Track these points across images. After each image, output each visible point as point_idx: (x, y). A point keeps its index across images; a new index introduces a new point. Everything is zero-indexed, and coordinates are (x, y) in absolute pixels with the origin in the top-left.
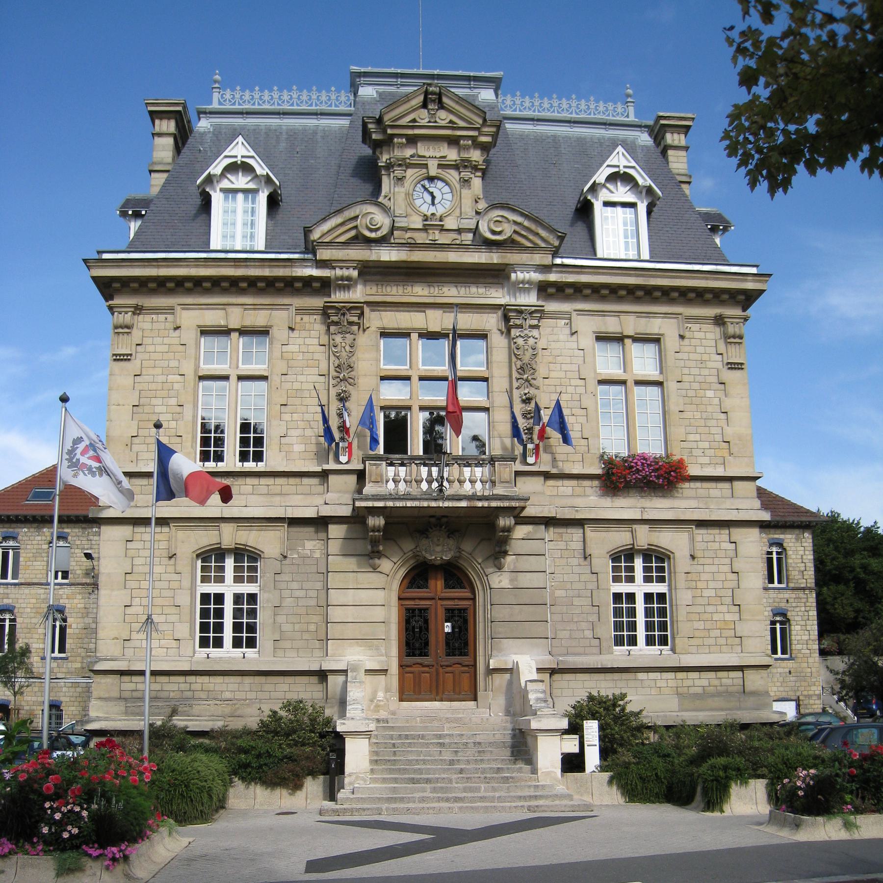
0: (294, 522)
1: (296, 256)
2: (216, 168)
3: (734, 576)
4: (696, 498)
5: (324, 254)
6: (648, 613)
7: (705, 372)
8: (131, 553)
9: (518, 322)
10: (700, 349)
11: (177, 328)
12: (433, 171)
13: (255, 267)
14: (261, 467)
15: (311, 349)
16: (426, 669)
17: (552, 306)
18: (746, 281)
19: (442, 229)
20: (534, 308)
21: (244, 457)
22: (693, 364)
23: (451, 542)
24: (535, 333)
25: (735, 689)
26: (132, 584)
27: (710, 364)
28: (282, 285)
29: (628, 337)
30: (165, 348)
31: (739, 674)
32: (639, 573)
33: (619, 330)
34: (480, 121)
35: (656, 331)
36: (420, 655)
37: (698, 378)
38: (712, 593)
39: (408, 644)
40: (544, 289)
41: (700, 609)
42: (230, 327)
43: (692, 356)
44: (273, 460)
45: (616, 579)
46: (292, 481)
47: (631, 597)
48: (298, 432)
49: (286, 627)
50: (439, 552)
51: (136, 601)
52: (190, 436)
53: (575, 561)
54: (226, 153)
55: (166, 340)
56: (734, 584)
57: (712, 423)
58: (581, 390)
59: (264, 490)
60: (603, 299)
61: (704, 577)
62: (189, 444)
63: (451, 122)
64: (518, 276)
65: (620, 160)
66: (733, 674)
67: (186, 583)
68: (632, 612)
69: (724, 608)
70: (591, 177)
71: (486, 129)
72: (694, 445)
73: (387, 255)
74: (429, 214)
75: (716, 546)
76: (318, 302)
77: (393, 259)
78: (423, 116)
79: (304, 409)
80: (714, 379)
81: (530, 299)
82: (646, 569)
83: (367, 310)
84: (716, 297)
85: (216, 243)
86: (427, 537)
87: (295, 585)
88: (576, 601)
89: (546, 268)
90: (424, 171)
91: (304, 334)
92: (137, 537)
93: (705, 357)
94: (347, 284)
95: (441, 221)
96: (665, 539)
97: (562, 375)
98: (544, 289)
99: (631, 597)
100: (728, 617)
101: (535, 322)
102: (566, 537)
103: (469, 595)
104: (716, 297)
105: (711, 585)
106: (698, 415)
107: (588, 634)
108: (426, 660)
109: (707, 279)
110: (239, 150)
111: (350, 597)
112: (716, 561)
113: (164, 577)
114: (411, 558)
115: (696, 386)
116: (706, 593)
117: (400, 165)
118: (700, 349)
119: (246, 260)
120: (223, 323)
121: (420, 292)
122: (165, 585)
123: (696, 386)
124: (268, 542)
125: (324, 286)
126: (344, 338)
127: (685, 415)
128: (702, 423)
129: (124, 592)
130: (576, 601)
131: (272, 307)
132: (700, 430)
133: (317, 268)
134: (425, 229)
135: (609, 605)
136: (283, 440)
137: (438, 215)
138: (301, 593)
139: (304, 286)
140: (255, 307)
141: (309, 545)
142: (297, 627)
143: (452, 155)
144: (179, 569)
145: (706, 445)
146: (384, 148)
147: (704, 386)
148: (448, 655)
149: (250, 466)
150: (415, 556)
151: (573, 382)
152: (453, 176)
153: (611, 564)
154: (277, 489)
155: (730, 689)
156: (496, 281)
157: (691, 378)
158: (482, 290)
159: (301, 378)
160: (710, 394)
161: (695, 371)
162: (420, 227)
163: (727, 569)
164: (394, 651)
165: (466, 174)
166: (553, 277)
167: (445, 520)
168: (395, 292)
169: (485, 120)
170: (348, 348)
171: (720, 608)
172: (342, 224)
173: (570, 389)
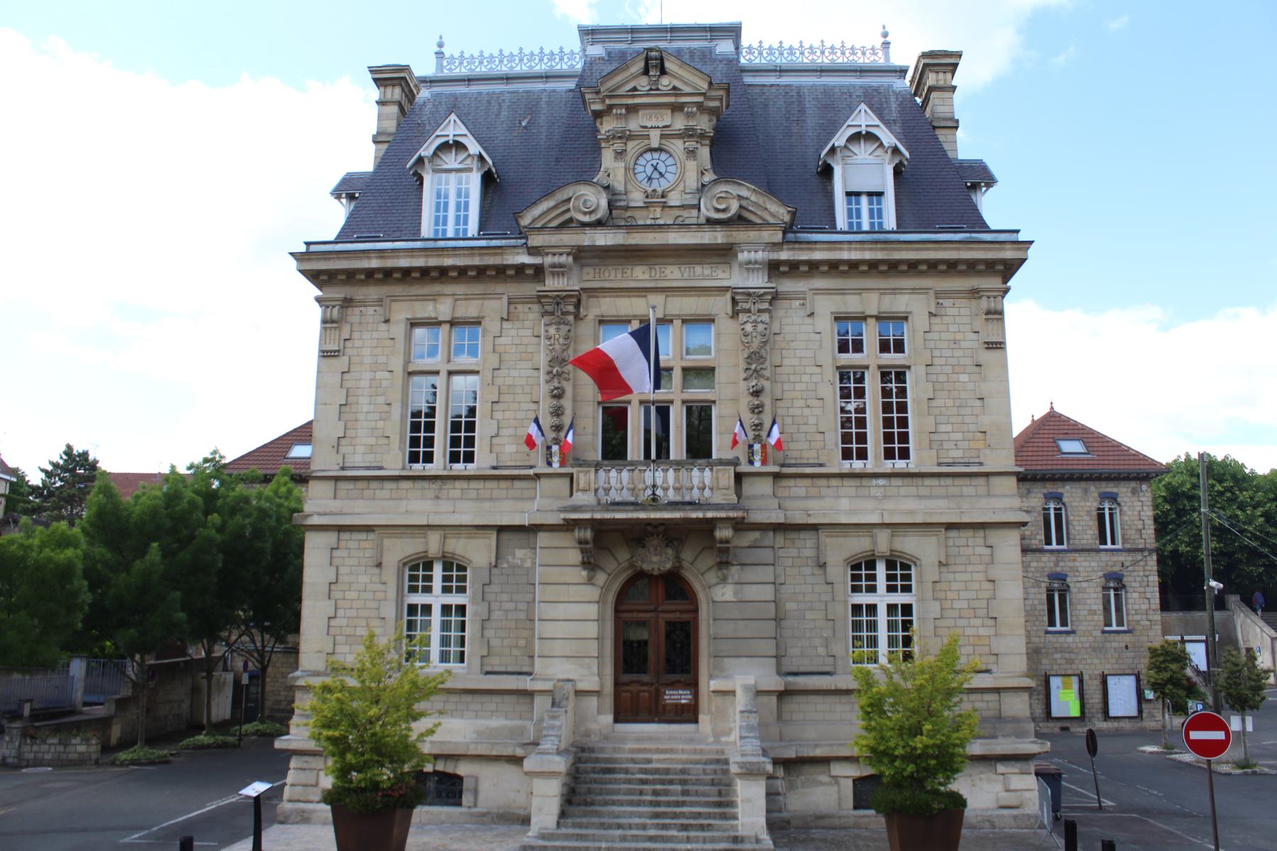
0: (501, 529)
1: (503, 242)
2: (427, 150)
3: (989, 585)
4: (947, 497)
5: (536, 240)
6: (891, 626)
7: (958, 353)
8: (336, 561)
9: (747, 306)
10: (952, 328)
11: (387, 321)
12: (655, 144)
13: (464, 255)
14: (471, 468)
15: (525, 341)
16: (645, 688)
17: (787, 285)
18: (1004, 249)
19: (665, 206)
20: (762, 291)
21: (454, 458)
22: (945, 345)
23: (670, 551)
24: (765, 317)
25: (991, 713)
26: (336, 595)
27: (964, 344)
28: (494, 273)
29: (871, 316)
30: (375, 343)
31: (994, 697)
32: (881, 582)
33: (860, 310)
34: (705, 86)
35: (902, 309)
36: (638, 672)
37: (951, 361)
38: (964, 605)
39: (625, 660)
40: (774, 268)
41: (950, 622)
42: (440, 319)
43: (944, 336)
44: (483, 461)
45: (856, 589)
46: (503, 484)
47: (872, 609)
48: (511, 431)
49: (494, 642)
50: (657, 561)
51: (341, 613)
52: (398, 437)
53: (807, 571)
54: (438, 133)
55: (375, 335)
56: (988, 594)
57: (968, 411)
58: (815, 378)
59: (473, 494)
60: (844, 274)
61: (955, 586)
62: (397, 445)
63: (675, 88)
64: (743, 256)
65: (864, 119)
66: (987, 697)
67: (392, 593)
68: (873, 626)
69: (978, 622)
70: (830, 140)
71: (713, 93)
72: (945, 437)
73: (603, 238)
74: (649, 190)
75: (969, 551)
76: (531, 289)
77: (609, 243)
78: (643, 83)
79: (516, 406)
80: (968, 361)
81: (758, 281)
82: (890, 578)
83: (584, 297)
84: (972, 267)
85: (427, 229)
86: (644, 546)
87: (505, 597)
88: (809, 615)
89: (775, 246)
90: (646, 142)
91: (518, 324)
92: (343, 544)
93: (959, 336)
94: (559, 270)
95: (663, 197)
96: (909, 545)
97: (796, 362)
98: (774, 268)
99: (872, 609)
100: (982, 631)
101: (765, 306)
102: (799, 543)
103: (691, 607)
104: (972, 267)
105: (964, 595)
106: (950, 403)
107: (821, 651)
108: (645, 678)
109: (959, 249)
110: (453, 128)
111: (561, 611)
112: (970, 568)
113: (370, 587)
114: (628, 568)
115: (948, 369)
116: (957, 605)
117: (620, 138)
118: (952, 328)
119: (455, 248)
120: (433, 315)
121: (640, 274)
122: (369, 595)
123: (948, 369)
124: (478, 552)
125: (538, 273)
126: (558, 330)
127: (934, 403)
128: (955, 411)
129: (328, 602)
130: (809, 615)
131: (484, 296)
132: (951, 420)
133: (530, 254)
134: (647, 206)
135: (846, 618)
136: (495, 441)
137: (660, 190)
138: (511, 606)
139: (517, 273)
140: (467, 298)
141: (520, 553)
142: (506, 642)
143: (679, 123)
144: (384, 578)
145: (960, 436)
146: (605, 119)
147: (957, 369)
148: (669, 672)
149: (459, 467)
150: (632, 566)
151: (808, 370)
152: (678, 146)
153: (850, 572)
154: (487, 494)
155: (985, 714)
156: (723, 260)
157: (942, 361)
158: (707, 271)
159: (514, 373)
160: (964, 378)
161: (949, 353)
162: (641, 204)
163: (981, 576)
164: (609, 670)
165: (691, 144)
166: (784, 255)
167: (662, 528)
168: (613, 276)
169: (711, 84)
170: (561, 341)
171: (973, 622)
172: (556, 207)
173: (805, 378)
